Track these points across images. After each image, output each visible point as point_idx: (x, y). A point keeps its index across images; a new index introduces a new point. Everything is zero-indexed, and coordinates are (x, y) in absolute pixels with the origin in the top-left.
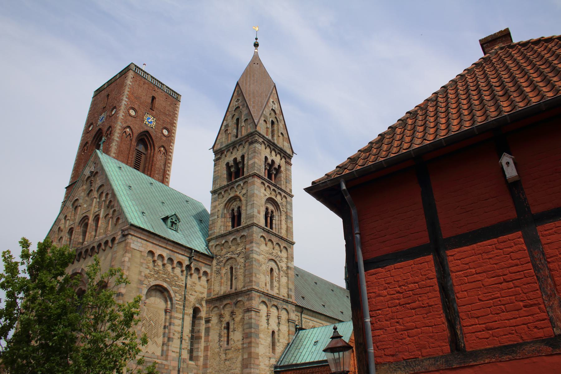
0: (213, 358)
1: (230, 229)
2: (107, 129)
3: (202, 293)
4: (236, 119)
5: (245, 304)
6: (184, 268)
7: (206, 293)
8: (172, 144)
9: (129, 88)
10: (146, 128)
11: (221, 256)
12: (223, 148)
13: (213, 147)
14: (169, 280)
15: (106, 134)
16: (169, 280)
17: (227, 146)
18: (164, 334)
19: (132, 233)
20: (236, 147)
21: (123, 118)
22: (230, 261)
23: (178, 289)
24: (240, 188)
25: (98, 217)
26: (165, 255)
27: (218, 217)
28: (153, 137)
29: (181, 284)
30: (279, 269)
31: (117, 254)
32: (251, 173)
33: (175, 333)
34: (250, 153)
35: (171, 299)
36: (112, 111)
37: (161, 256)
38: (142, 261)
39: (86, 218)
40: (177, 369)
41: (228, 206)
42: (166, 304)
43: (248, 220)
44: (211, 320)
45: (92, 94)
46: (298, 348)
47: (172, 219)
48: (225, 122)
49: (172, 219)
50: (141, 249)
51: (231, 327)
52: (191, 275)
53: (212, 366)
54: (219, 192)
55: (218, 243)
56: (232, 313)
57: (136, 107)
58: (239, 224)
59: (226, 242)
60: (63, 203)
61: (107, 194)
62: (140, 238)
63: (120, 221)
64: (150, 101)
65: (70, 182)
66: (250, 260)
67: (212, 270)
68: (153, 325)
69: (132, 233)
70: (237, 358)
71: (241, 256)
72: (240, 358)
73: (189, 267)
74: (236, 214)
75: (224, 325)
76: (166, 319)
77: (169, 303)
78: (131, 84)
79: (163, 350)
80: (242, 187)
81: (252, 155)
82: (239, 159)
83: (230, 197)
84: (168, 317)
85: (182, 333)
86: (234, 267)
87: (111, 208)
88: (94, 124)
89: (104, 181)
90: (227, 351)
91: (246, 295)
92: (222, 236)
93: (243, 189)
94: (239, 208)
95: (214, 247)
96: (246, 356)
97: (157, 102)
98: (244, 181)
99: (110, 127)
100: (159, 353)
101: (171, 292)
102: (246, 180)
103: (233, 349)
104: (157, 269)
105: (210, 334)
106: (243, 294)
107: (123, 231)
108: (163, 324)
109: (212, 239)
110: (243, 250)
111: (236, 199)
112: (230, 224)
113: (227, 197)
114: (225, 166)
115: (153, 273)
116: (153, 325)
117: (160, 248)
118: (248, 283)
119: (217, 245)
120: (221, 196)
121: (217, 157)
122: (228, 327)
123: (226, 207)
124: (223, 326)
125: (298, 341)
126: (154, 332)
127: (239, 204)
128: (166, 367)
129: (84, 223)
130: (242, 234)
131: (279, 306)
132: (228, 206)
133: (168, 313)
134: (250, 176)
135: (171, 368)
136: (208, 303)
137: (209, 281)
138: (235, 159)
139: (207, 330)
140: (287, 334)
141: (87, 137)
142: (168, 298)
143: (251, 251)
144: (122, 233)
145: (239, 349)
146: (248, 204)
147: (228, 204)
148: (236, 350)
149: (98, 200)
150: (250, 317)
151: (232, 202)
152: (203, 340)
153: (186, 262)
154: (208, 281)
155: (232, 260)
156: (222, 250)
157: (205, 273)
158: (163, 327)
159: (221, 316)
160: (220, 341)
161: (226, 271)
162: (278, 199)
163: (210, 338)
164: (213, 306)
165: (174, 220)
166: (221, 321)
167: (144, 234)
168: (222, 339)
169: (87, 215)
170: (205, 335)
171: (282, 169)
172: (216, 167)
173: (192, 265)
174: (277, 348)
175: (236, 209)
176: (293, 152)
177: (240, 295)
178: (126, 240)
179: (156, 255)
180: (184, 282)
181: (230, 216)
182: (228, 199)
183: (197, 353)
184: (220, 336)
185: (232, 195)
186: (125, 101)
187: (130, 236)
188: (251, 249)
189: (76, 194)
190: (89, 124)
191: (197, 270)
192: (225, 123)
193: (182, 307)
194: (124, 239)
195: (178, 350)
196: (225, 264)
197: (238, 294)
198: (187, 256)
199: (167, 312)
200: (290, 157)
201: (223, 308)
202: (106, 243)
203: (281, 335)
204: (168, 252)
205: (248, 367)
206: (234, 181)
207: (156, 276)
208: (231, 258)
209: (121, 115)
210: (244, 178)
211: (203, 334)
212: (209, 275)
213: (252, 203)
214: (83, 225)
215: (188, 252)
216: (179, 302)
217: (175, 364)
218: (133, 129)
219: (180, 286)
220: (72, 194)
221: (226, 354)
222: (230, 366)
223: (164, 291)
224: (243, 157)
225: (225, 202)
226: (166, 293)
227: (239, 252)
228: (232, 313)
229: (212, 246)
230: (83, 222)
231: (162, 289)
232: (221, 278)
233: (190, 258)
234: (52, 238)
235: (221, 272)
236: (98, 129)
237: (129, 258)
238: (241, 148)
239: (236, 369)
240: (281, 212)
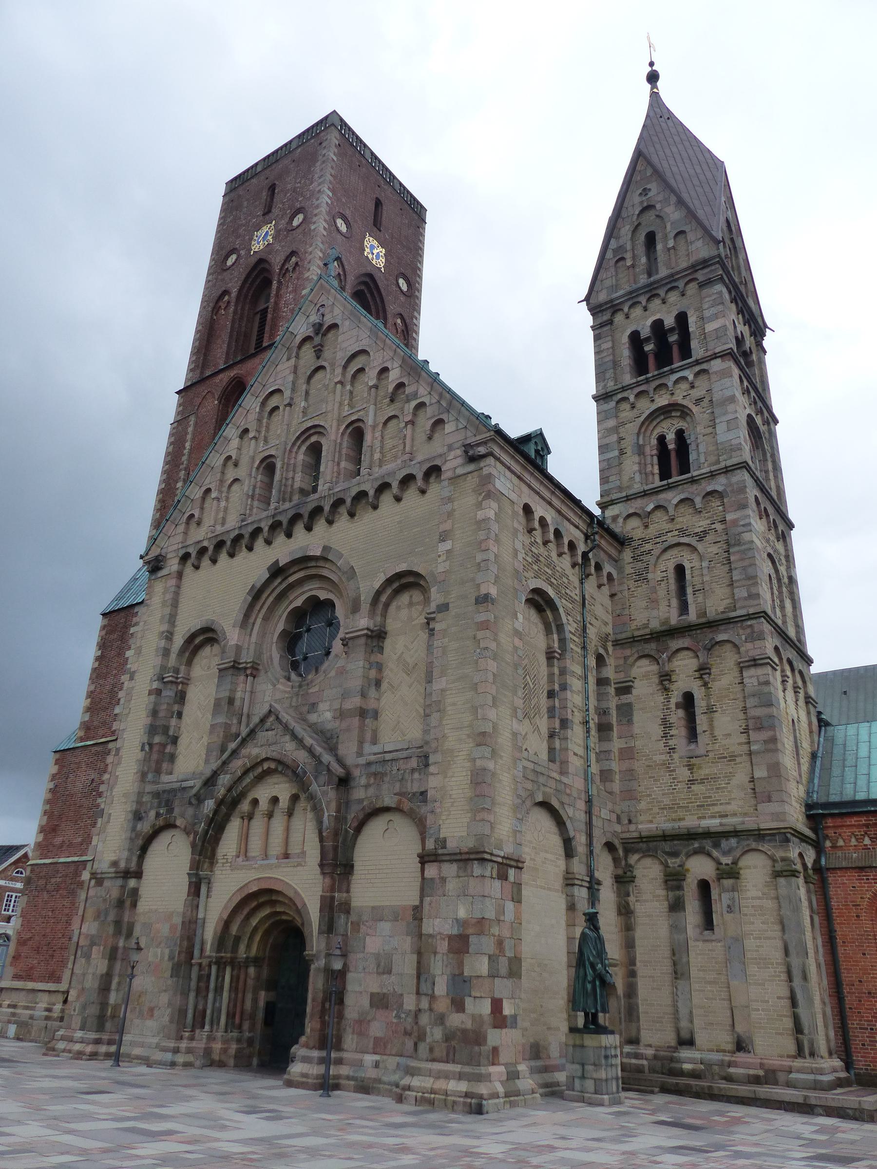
0: (650, 778)
1: (657, 483)
2: (283, 258)
3: (606, 624)
4: (644, 234)
5: (742, 649)
6: (580, 561)
7: (611, 626)
8: (416, 314)
9: (332, 168)
10: (369, 269)
11: (645, 541)
12: (617, 298)
13: (587, 299)
14: (555, 582)
15: (281, 269)
16: (555, 582)
17: (631, 293)
18: (551, 711)
19: (497, 451)
20: (657, 295)
21: (325, 233)
22: (674, 552)
23: (571, 606)
24: (684, 386)
25: (356, 425)
26: (549, 520)
27: (622, 453)
28: (382, 290)
29: (573, 595)
30: (779, 580)
31: (456, 503)
32: (717, 350)
33: (574, 709)
34: (705, 306)
35: (560, 628)
36: (292, 219)
37: (542, 521)
38: (516, 525)
39: (312, 431)
40: (583, 796)
41: (646, 430)
42: (547, 639)
43: (725, 457)
44: (631, 687)
45: (222, 190)
46: (848, 763)
47: (536, 443)
48: (613, 241)
49: (536, 443)
50: (513, 496)
51: (700, 704)
52: (588, 576)
53: (649, 795)
54: (620, 396)
55: (631, 511)
56: (703, 671)
57: (348, 213)
58: (685, 467)
59: (657, 507)
60: (176, 424)
61: (384, 370)
62: (509, 468)
63: (449, 428)
64: (371, 206)
65: (187, 380)
66: (743, 547)
67: (620, 570)
68: (532, 686)
69: (497, 451)
70: (729, 776)
71: (710, 538)
72: (741, 777)
73: (585, 555)
74: (671, 446)
75: (676, 697)
76: (551, 675)
77: (555, 636)
78: (335, 159)
79: (551, 750)
80: (692, 383)
81: (713, 310)
82: (669, 321)
83: (654, 407)
84: (556, 671)
85: (587, 710)
86: (687, 566)
87: (408, 401)
88: (243, 252)
89: (364, 342)
90: (693, 761)
91: (743, 628)
92: (645, 494)
93: (693, 387)
94: (680, 434)
95: (621, 520)
96: (761, 773)
97: (384, 212)
98: (697, 368)
99: (293, 253)
100: (544, 756)
101: (561, 610)
102: (704, 366)
103: (711, 755)
104: (536, 551)
105: (636, 718)
106: (732, 626)
107: (467, 447)
108: (546, 688)
109: (612, 503)
110: (713, 526)
111: (670, 411)
112: (656, 470)
113: (646, 407)
114: (625, 339)
115: (530, 560)
116: (532, 686)
117: (541, 500)
118: (745, 599)
119: (629, 516)
120: (625, 406)
121: (599, 321)
122: (688, 700)
123: (643, 430)
124: (673, 701)
125: (838, 751)
126: (533, 703)
127: (681, 424)
128: (568, 791)
129: (308, 443)
130: (709, 488)
131: (795, 663)
132: (646, 430)
133: (556, 661)
134: (716, 358)
135: (575, 794)
136: (618, 647)
137: (616, 598)
138: (658, 325)
139: (626, 711)
140: (807, 731)
141: (222, 280)
142: (553, 625)
143: (743, 526)
144: (466, 452)
145: (735, 756)
146: (717, 421)
147: (647, 423)
148: (726, 757)
149: (348, 387)
150: (762, 679)
151: (658, 420)
152: (615, 733)
153: (581, 548)
154: (612, 596)
155: (680, 548)
156: (646, 527)
157: (610, 576)
158: (545, 694)
159: (665, 679)
160: (665, 735)
161: (664, 574)
162: (758, 420)
163: (637, 729)
164: (636, 656)
165: (539, 448)
166: (666, 689)
167: (517, 461)
168: (672, 733)
169: (316, 423)
170: (619, 722)
171: (754, 357)
172: (599, 342)
173: (590, 555)
174: (802, 761)
175: (671, 437)
176: (766, 326)
177: (722, 627)
178: (482, 469)
179: (537, 517)
180: (577, 591)
181: (655, 452)
182: (647, 412)
183: (607, 762)
184: (666, 724)
185: (662, 400)
186: (325, 198)
187: (490, 460)
188: (742, 523)
189: (271, 380)
190: (224, 253)
191: (598, 567)
192: (613, 244)
193: (579, 650)
194: (471, 467)
195: (581, 751)
196: (658, 558)
197: (712, 625)
198: (581, 531)
199: (554, 657)
200: (763, 335)
201: (670, 659)
202: (408, 480)
203: (802, 733)
204: (553, 512)
205: (773, 799)
206: (656, 373)
207: (536, 567)
208: (679, 544)
209: (320, 225)
210: (697, 362)
211: (614, 721)
212: (616, 583)
213: (730, 417)
214: (304, 448)
215: (584, 521)
216: (575, 638)
217: (578, 783)
218: (345, 263)
219: (573, 601)
220: (259, 379)
221: (690, 767)
222: (710, 797)
223: (545, 607)
224: (682, 319)
225: (642, 419)
226: (549, 613)
227: (702, 529)
228: (703, 671)
229: (615, 518)
230: (303, 442)
231: (542, 603)
232: (654, 590)
233: (587, 537)
234: (207, 481)
235: (650, 576)
236: (253, 260)
237: (496, 514)
238: (675, 298)
239: (728, 803)
240: (764, 454)
